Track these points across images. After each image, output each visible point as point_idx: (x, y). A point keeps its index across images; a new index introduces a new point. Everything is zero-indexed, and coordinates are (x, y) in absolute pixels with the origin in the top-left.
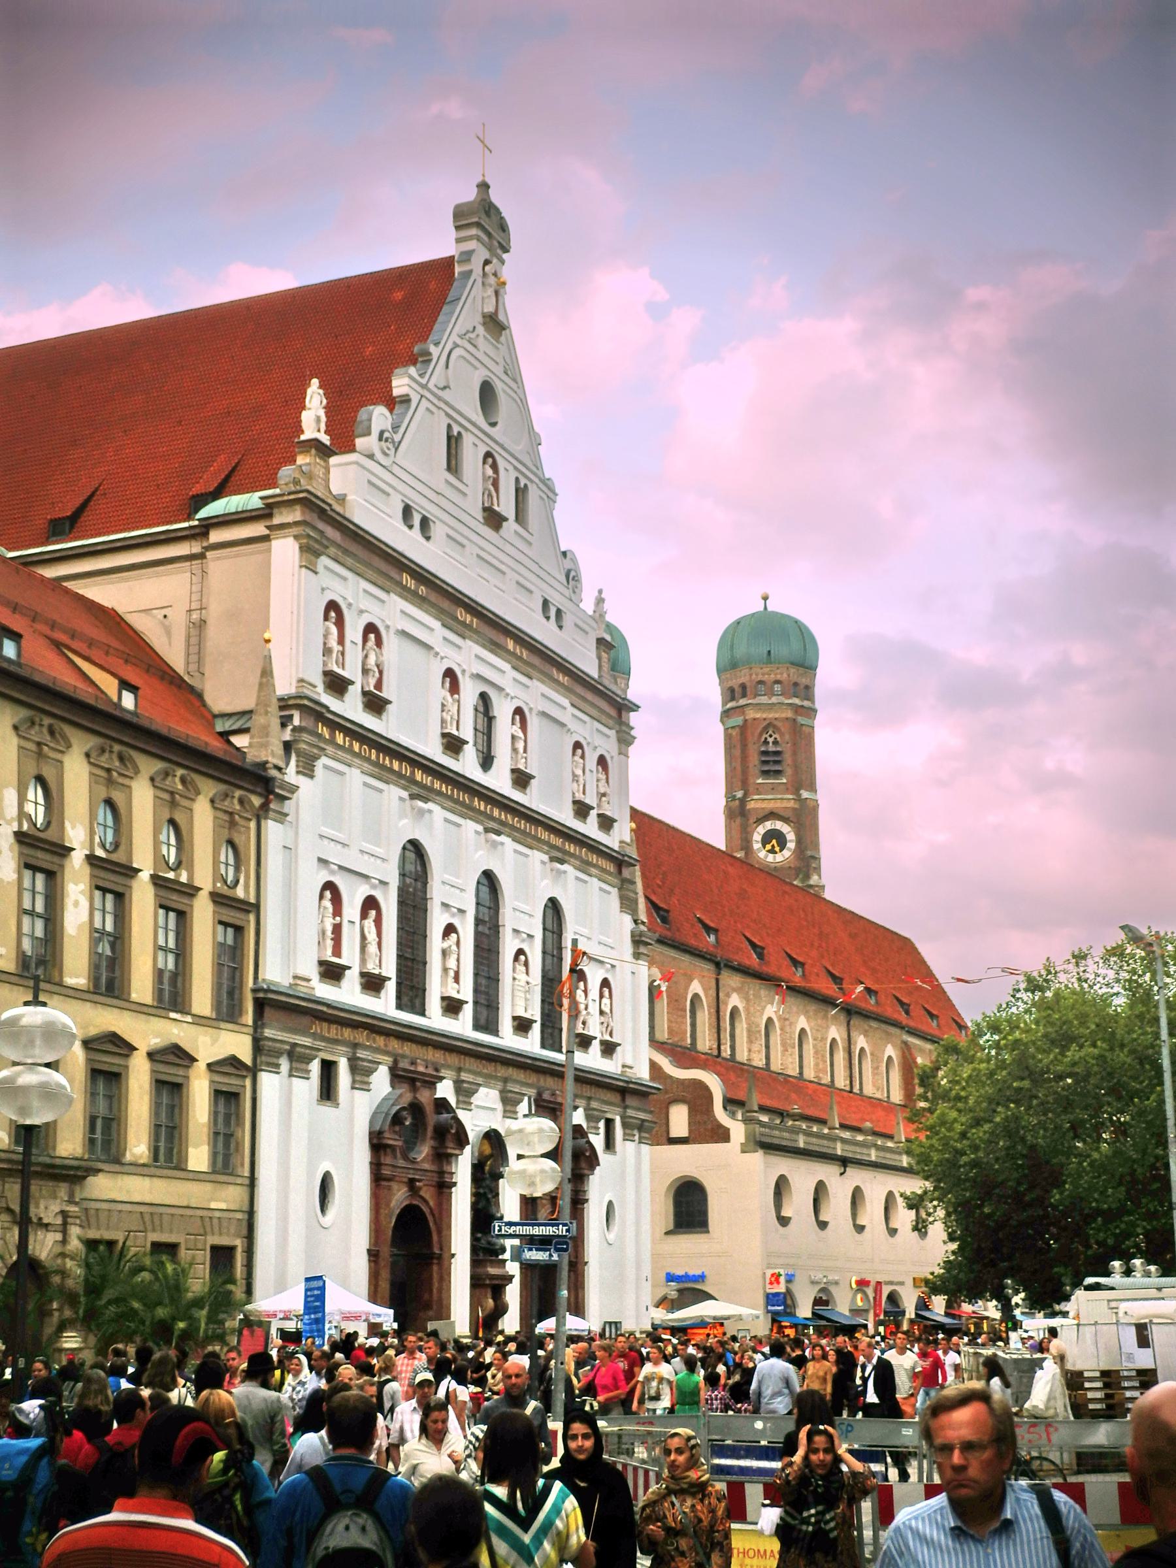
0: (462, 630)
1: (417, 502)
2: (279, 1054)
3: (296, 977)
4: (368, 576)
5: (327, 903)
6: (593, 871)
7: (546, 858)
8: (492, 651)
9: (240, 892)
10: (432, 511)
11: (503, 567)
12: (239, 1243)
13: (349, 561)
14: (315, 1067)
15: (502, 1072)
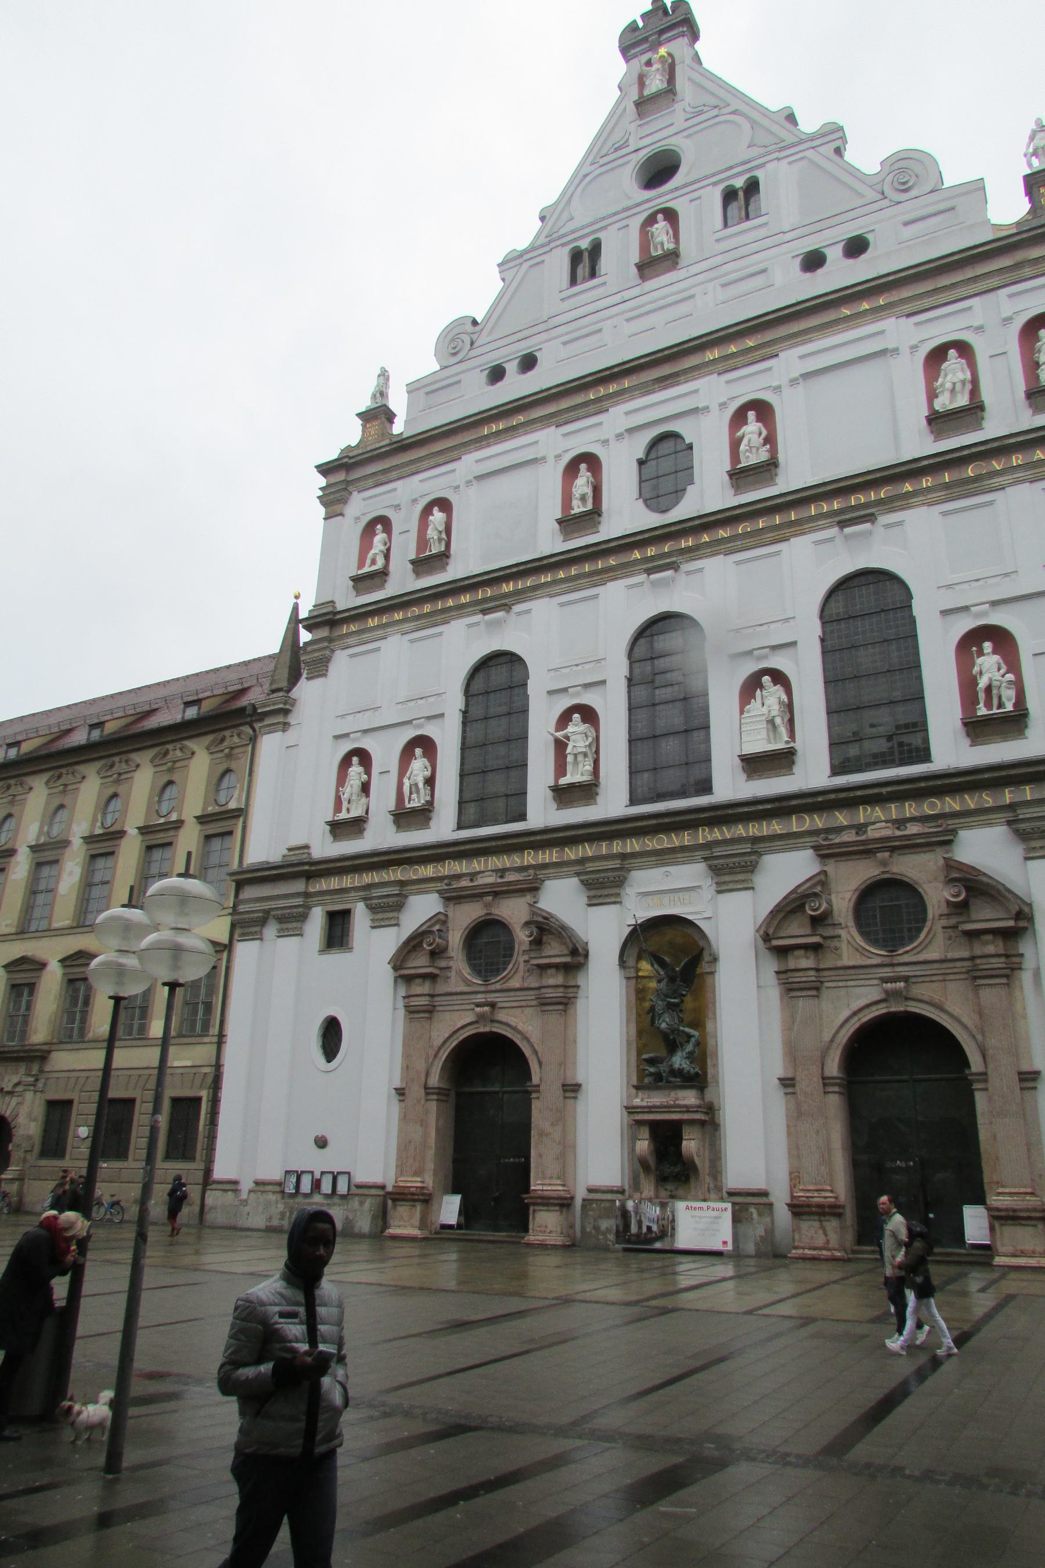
0: (599, 406)
1: (493, 359)
2: (263, 922)
3: (290, 850)
4: (423, 467)
5: (356, 770)
6: (997, 481)
7: (834, 531)
8: (665, 388)
9: (233, 805)
10: (524, 348)
11: (686, 294)
12: (204, 1094)
13: (394, 475)
14: (316, 922)
15: (704, 835)
